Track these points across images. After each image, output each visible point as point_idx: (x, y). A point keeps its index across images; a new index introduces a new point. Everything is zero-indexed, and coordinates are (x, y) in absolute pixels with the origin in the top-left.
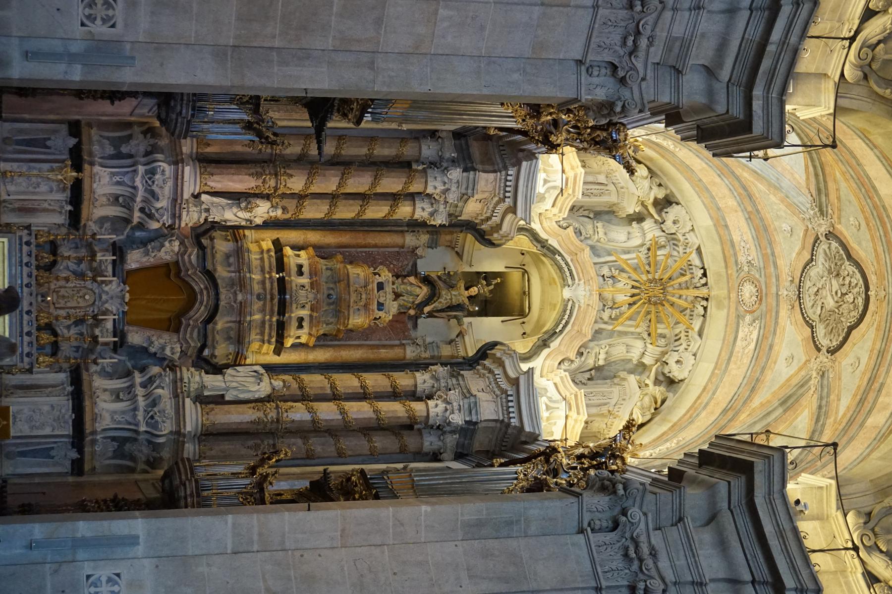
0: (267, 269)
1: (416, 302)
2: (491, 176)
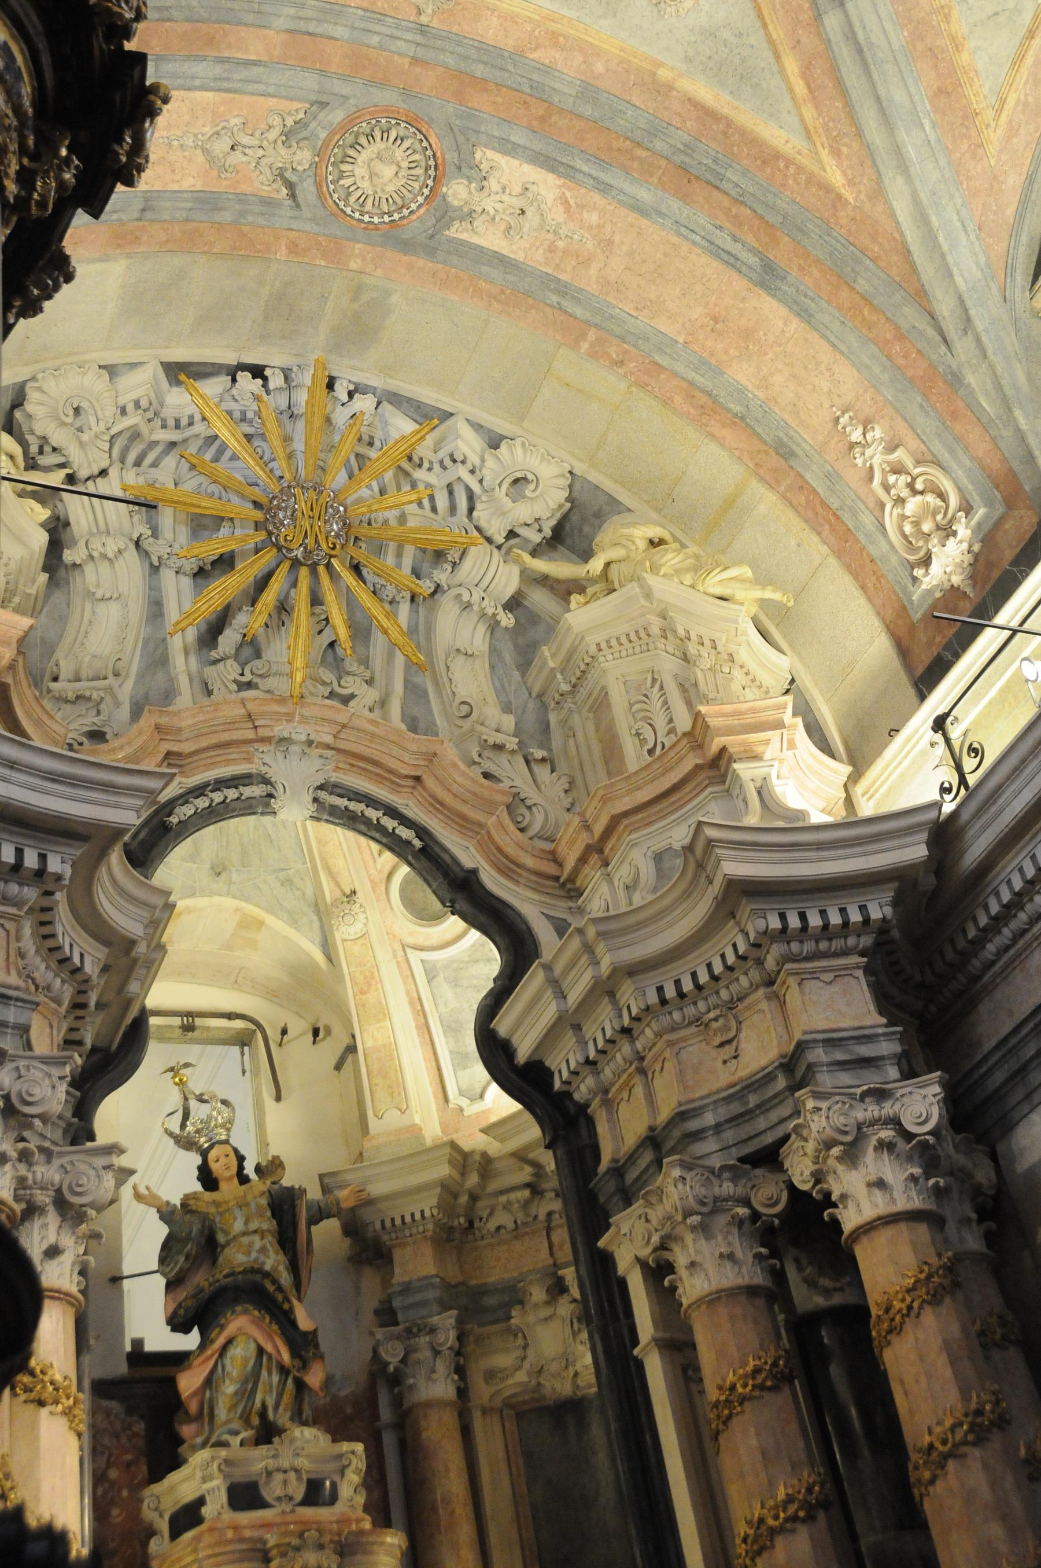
1: (286, 1356)
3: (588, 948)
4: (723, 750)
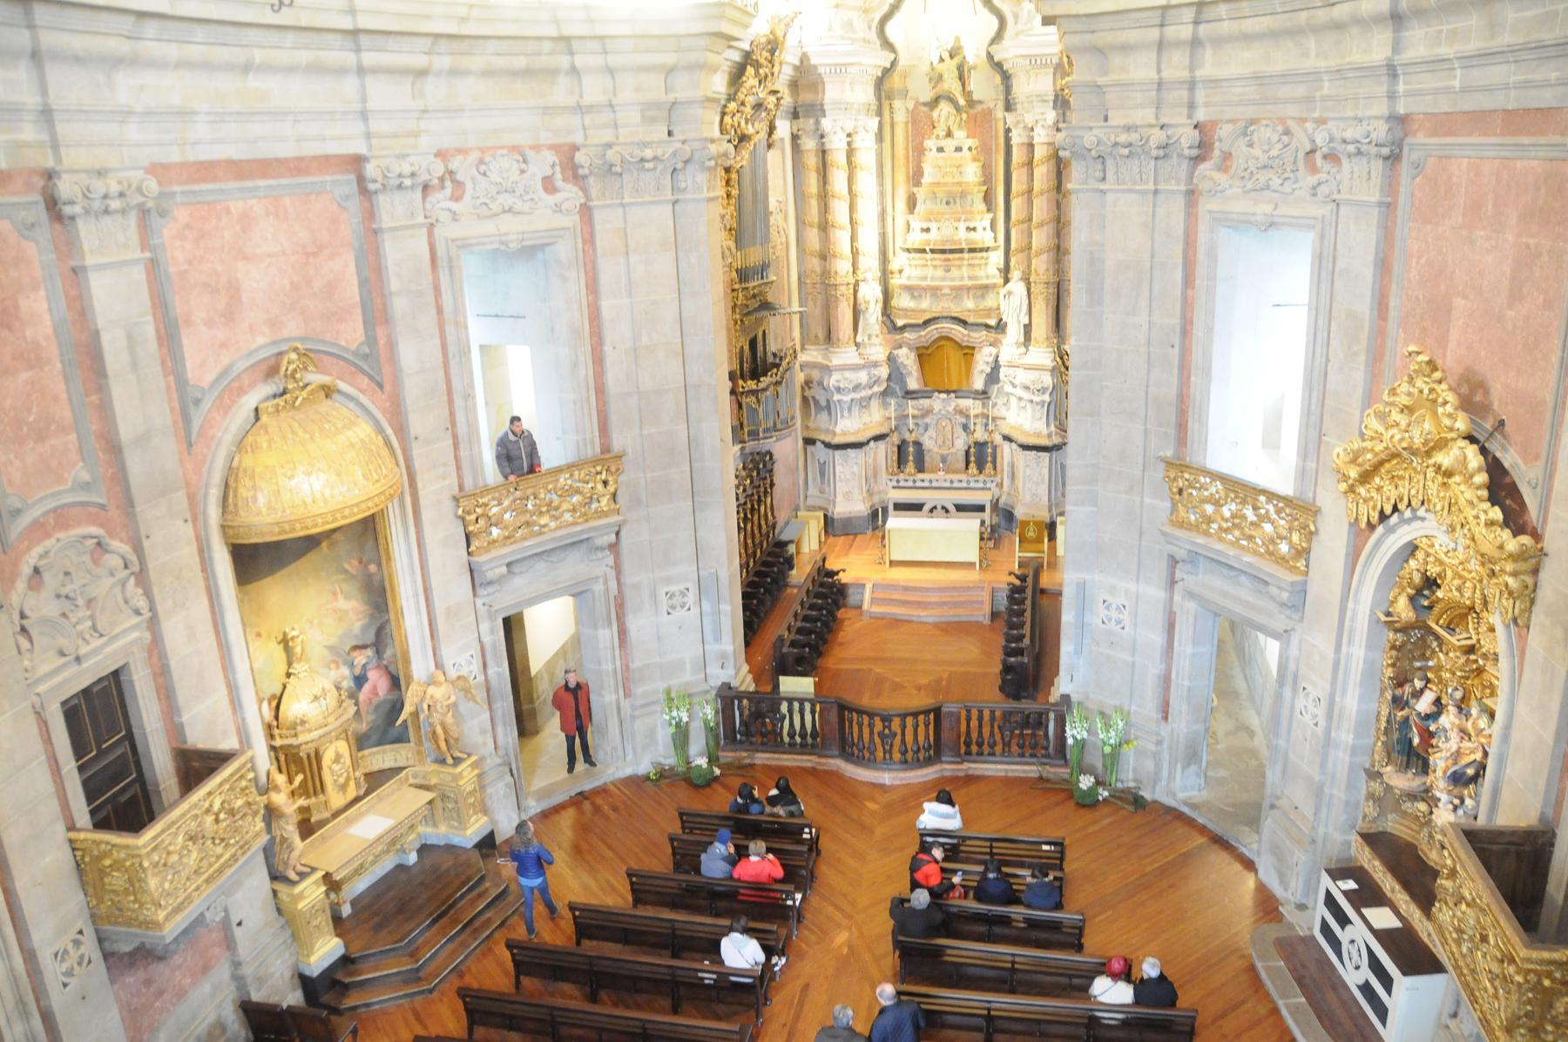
0: (922, 262)
2: (828, 87)
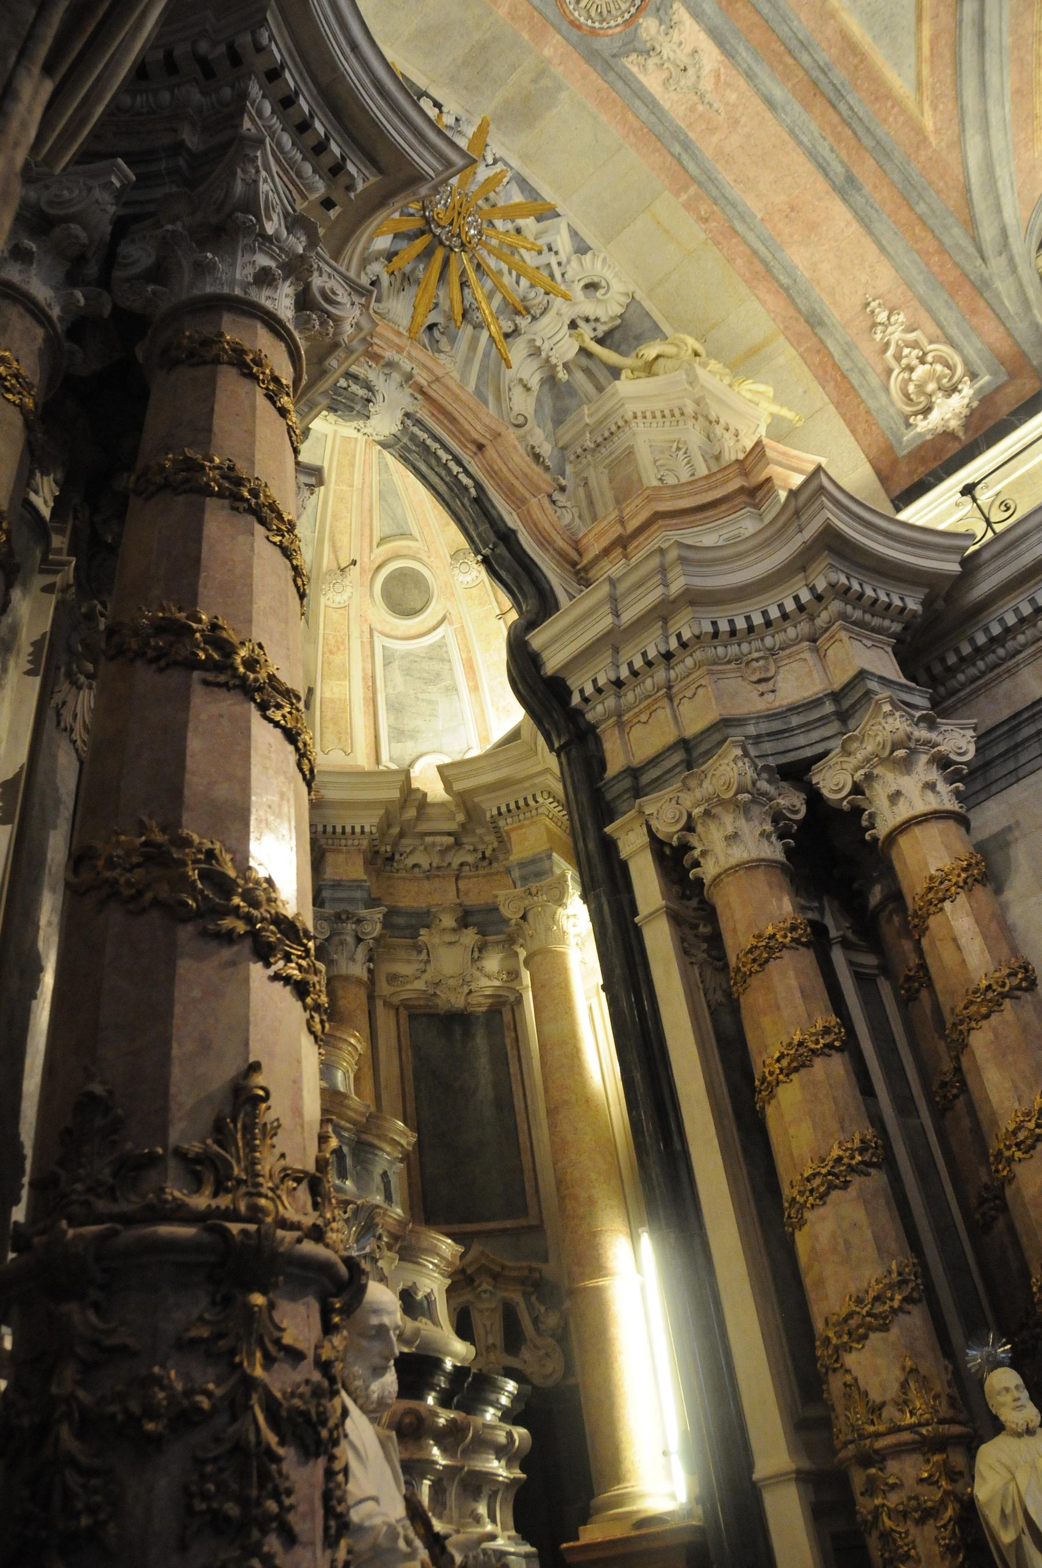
3: (663, 570)
4: (769, 480)
